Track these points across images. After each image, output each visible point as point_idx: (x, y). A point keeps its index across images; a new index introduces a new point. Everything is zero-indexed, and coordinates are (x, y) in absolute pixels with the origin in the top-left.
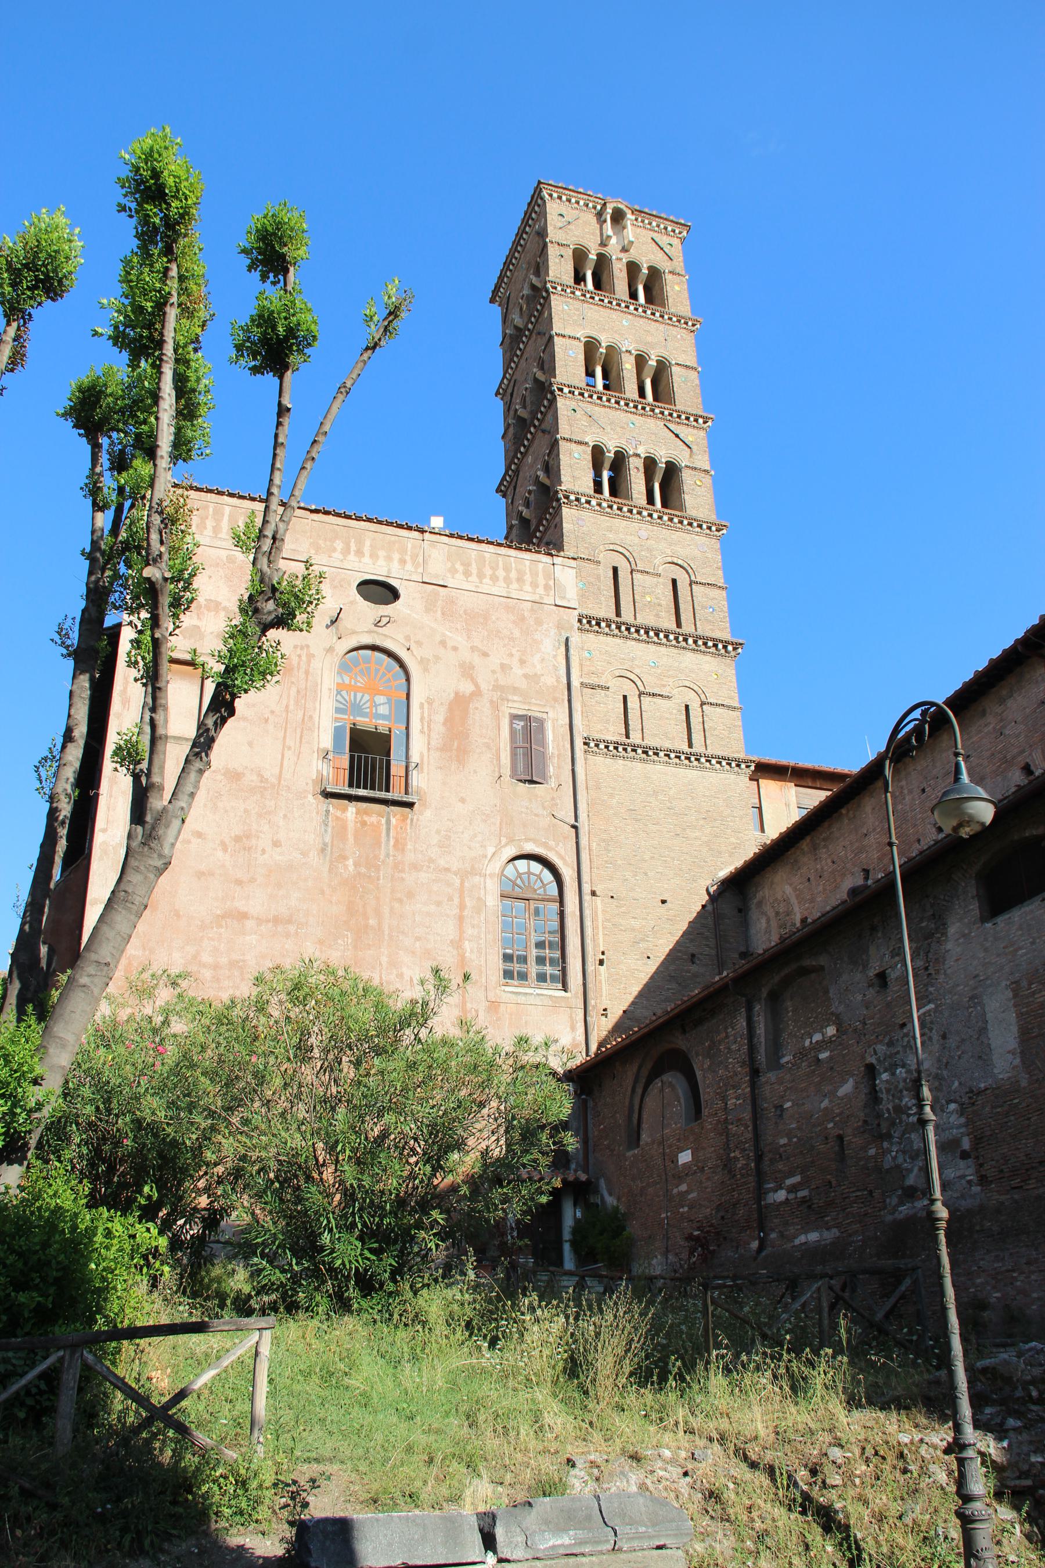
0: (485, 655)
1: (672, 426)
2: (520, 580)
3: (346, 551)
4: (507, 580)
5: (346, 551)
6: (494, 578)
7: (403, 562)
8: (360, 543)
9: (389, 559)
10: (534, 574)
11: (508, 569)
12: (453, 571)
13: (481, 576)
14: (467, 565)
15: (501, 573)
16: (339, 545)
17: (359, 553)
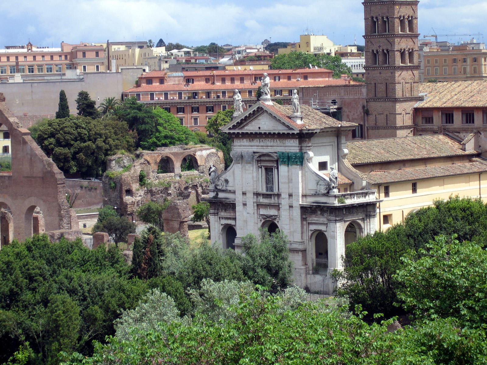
0: (351, 112)
1: (388, 39)
2: (356, 93)
3: (329, 95)
4: (354, 94)
5: (329, 95)
6: (352, 94)
7: (337, 94)
8: (331, 92)
9: (335, 94)
10: (358, 91)
11: (354, 91)
12: (345, 94)
13: (350, 94)
14: (347, 92)
15: (353, 92)
16: (328, 93)
17: (331, 94)
